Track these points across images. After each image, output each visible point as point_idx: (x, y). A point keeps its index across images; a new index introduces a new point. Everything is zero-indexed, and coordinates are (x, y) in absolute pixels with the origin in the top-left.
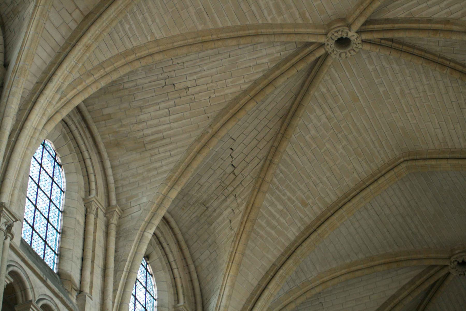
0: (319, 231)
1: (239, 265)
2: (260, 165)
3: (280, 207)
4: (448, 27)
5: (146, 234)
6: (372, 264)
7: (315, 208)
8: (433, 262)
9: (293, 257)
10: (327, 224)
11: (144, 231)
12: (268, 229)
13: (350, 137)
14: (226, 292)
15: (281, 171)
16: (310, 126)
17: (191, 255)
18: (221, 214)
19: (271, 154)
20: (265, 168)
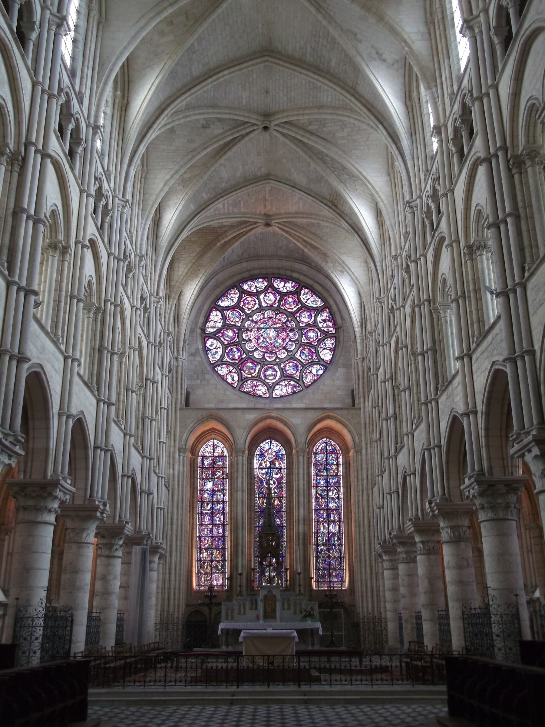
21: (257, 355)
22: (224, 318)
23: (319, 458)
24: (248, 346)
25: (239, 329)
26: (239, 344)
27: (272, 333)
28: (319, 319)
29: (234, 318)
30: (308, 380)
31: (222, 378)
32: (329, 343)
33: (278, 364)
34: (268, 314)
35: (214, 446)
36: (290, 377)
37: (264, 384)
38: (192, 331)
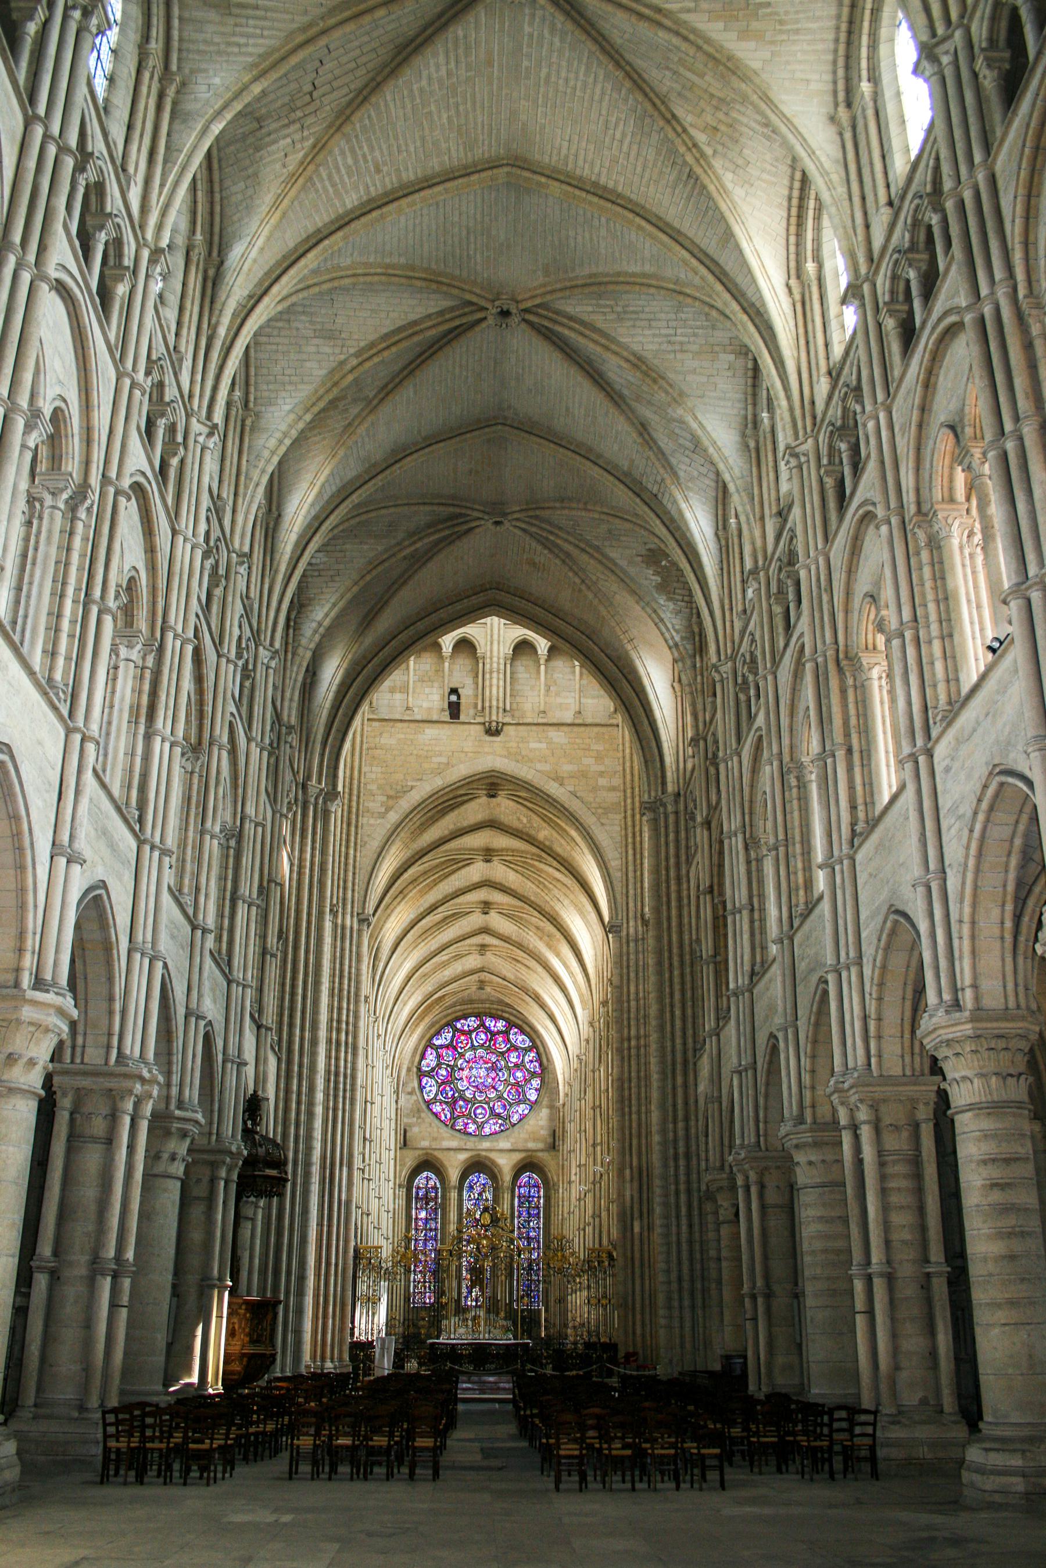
0: (385, 210)
1: (284, 214)
2: (347, 98)
3: (350, 161)
4: (658, 17)
5: (213, 127)
6: (411, 274)
7: (387, 179)
8: (475, 299)
9: (346, 230)
10: (395, 204)
11: (210, 122)
12: (327, 183)
13: (461, 108)
14: (260, 243)
15: (369, 117)
16: (425, 73)
17: (221, 181)
18: (275, 142)
19: (368, 89)
20: (354, 105)
21: (468, 1094)
22: (439, 1056)
23: (522, 1191)
24: (462, 1085)
25: (452, 1067)
26: (450, 1079)
27: (483, 1073)
28: (527, 1059)
29: (448, 1056)
30: (515, 1118)
31: (436, 1115)
32: (536, 1083)
33: (487, 1103)
34: (480, 1052)
35: (428, 1179)
36: (499, 1115)
37: (475, 1122)
38: (409, 1070)
